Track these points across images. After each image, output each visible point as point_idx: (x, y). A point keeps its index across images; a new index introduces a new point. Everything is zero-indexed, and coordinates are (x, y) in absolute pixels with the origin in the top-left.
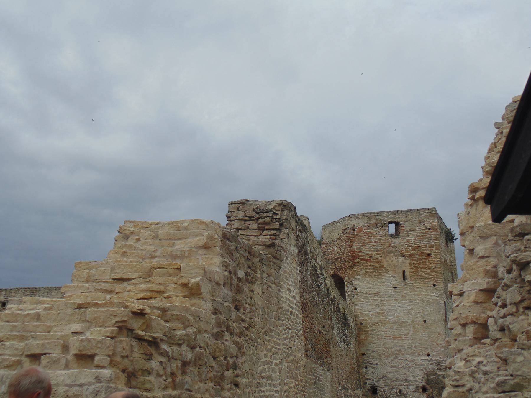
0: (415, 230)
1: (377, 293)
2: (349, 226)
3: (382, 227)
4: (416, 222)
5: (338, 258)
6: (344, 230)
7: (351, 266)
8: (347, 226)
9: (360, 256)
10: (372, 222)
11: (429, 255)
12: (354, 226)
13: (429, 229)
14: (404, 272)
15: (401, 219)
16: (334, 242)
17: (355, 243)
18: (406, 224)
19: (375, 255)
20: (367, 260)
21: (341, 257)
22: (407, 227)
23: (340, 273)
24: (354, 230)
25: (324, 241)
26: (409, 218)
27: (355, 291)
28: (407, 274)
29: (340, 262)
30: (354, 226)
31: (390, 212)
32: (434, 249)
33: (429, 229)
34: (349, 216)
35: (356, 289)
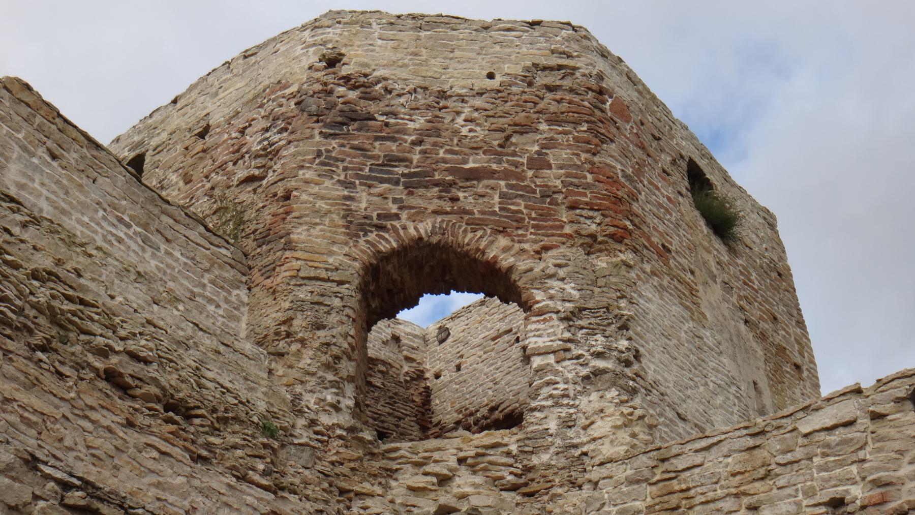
5: (475, 175)
21: (507, 175)
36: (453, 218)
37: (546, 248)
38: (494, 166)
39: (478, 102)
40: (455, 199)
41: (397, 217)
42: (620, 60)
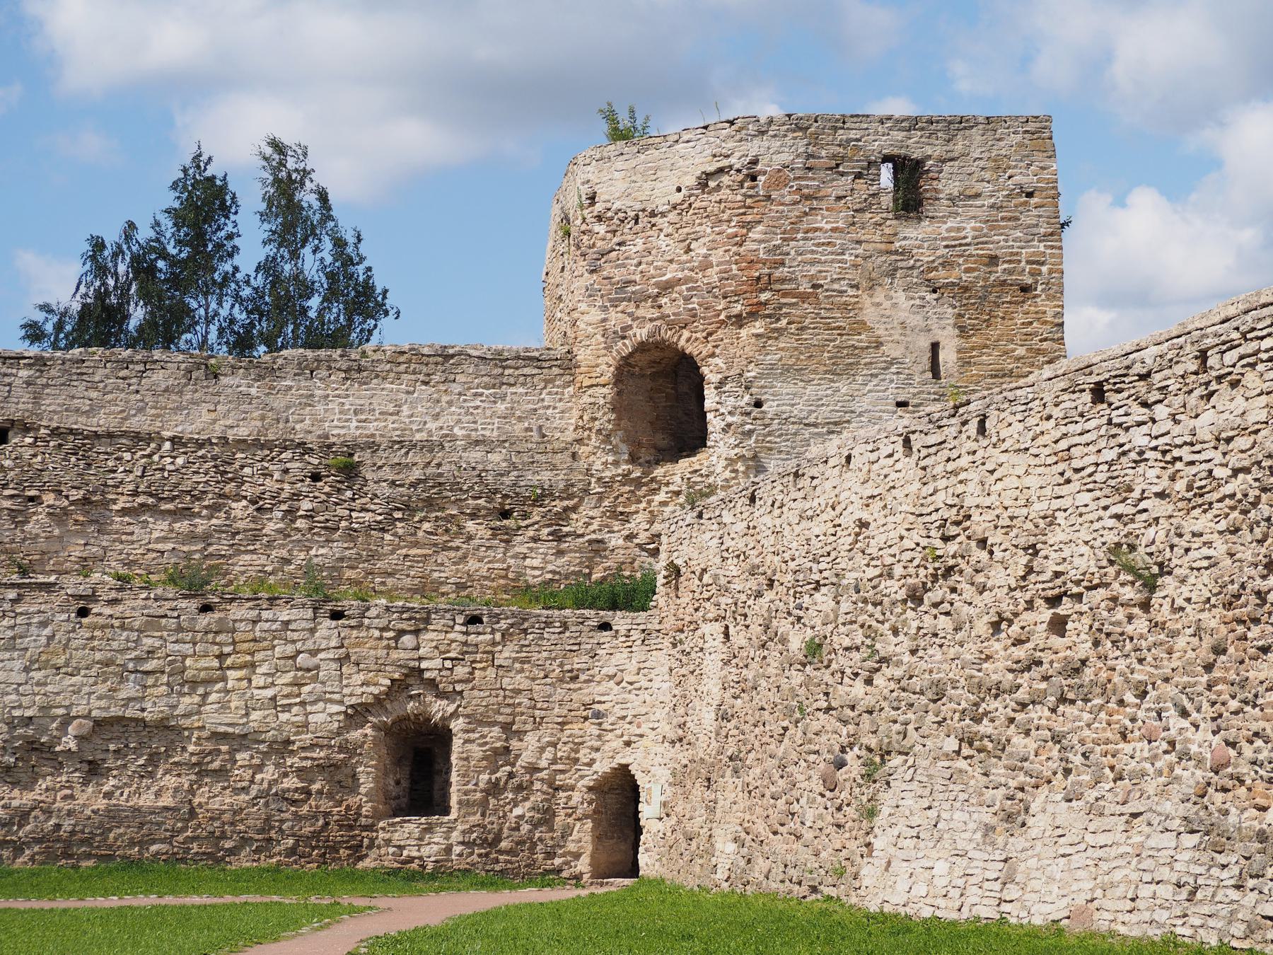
0: (977, 196)
1: (836, 424)
2: (733, 160)
3: (859, 176)
4: (982, 163)
6: (709, 175)
7: (739, 316)
8: (725, 163)
9: (783, 281)
10: (823, 153)
11: (1025, 289)
12: (755, 162)
13: (1030, 195)
14: (935, 347)
15: (929, 150)
16: (653, 214)
17: (760, 228)
18: (947, 168)
19: (833, 281)
20: (804, 297)
21: (687, 280)
22: (948, 184)
23: (686, 341)
24: (754, 178)
25: (599, 207)
26: (959, 147)
27: (756, 412)
28: (948, 357)
29: (687, 299)
30: (755, 162)
31: (889, 118)
32: (1044, 269)
33: (1030, 195)
34: (732, 123)
35: (758, 404)
36: (658, 323)
37: (710, 334)
38: (680, 275)
39: (672, 216)
40: (660, 307)
41: (630, 327)
42: (789, 116)
